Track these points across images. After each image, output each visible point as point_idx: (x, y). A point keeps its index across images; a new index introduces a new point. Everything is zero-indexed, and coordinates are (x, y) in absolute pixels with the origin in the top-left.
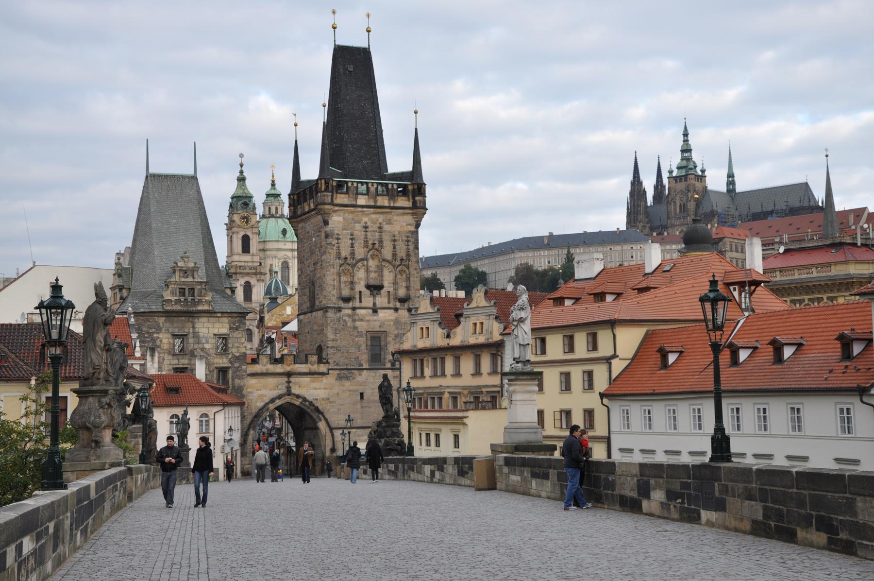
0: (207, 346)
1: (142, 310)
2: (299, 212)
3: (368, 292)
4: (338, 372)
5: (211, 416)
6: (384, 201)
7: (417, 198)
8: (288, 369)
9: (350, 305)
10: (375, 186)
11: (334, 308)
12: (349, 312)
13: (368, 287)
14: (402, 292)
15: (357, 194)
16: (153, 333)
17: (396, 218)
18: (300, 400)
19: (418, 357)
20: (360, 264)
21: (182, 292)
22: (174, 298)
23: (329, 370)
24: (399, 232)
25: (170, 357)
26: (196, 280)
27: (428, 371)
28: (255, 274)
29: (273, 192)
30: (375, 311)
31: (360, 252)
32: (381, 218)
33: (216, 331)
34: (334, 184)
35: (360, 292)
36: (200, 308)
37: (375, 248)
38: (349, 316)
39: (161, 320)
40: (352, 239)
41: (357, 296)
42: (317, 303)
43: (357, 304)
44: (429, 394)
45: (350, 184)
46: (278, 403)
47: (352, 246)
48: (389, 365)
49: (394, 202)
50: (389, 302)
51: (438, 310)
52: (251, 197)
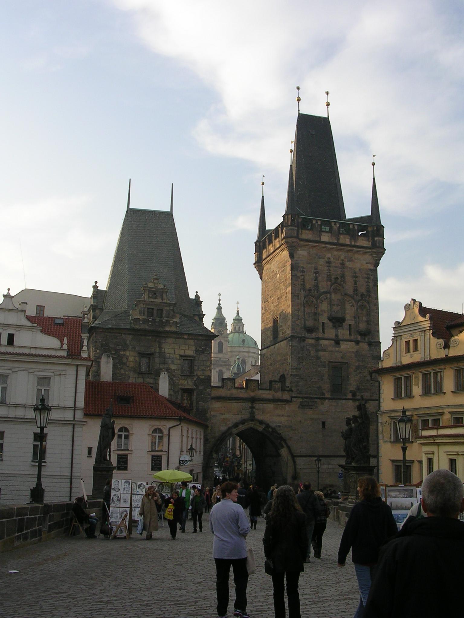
0: (173, 367)
1: (110, 326)
2: (264, 257)
3: (331, 324)
4: (301, 400)
5: (166, 432)
6: (345, 239)
7: (376, 239)
8: (252, 394)
9: (314, 335)
10: (338, 225)
11: (297, 337)
12: (313, 342)
13: (331, 319)
14: (362, 326)
15: (321, 231)
16: (120, 350)
17: (356, 256)
18: (263, 426)
19: (403, 374)
20: (323, 297)
21: (150, 312)
22: (142, 318)
23: (292, 397)
24: (360, 270)
25: (136, 375)
26: (164, 301)
27: (417, 390)
28: (226, 365)
29: (237, 318)
30: (337, 342)
31: (324, 285)
32: (343, 255)
33: (182, 353)
34: (300, 220)
35: (323, 323)
36: (167, 329)
37: (337, 282)
38: (312, 345)
39: (129, 338)
40: (316, 273)
41: (321, 328)
42: (281, 335)
43: (321, 335)
44: (419, 415)
45: (314, 222)
46: (242, 428)
47: (316, 279)
48: (350, 396)
49: (356, 240)
50: (350, 334)
51: (431, 318)
52: (225, 319)
